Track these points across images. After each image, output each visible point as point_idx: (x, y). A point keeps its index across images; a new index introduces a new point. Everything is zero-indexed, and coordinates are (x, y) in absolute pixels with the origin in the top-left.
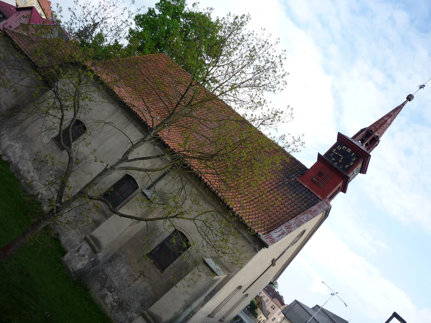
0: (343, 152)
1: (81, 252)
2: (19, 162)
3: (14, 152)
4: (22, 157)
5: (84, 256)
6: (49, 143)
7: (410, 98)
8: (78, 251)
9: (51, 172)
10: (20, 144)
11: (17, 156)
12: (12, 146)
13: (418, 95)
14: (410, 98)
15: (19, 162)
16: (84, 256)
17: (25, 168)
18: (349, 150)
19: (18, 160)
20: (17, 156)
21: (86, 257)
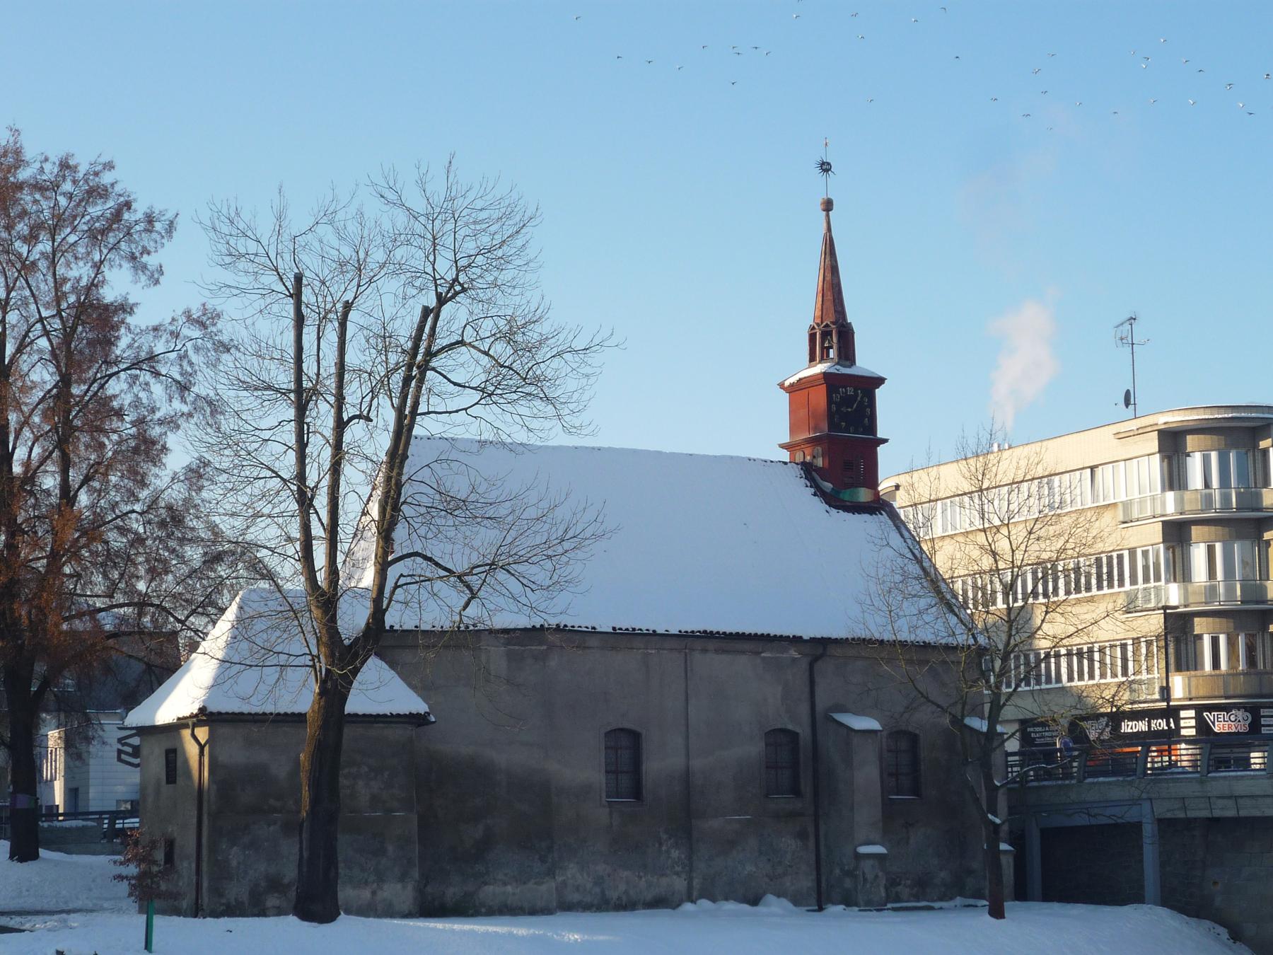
0: (848, 400)
1: (870, 876)
2: (603, 892)
3: (577, 888)
4: (599, 881)
5: (877, 876)
6: (611, 814)
7: (828, 206)
8: (865, 880)
9: (664, 848)
10: (571, 865)
11: (589, 886)
12: (564, 883)
13: (835, 187)
14: (828, 206)
15: (603, 892)
16: (877, 876)
17: (622, 887)
18: (850, 391)
19: (597, 890)
20: (589, 886)
21: (880, 874)
